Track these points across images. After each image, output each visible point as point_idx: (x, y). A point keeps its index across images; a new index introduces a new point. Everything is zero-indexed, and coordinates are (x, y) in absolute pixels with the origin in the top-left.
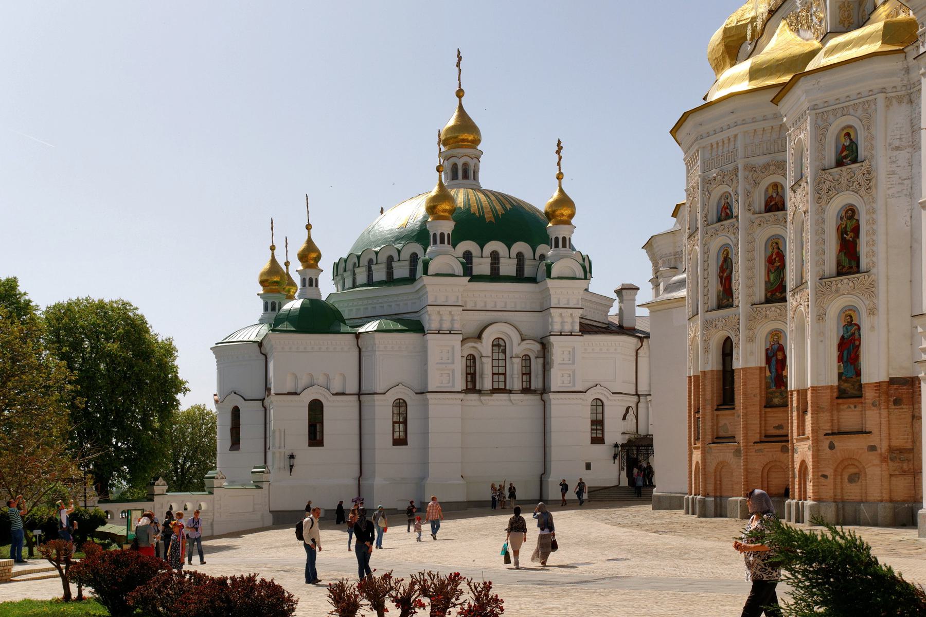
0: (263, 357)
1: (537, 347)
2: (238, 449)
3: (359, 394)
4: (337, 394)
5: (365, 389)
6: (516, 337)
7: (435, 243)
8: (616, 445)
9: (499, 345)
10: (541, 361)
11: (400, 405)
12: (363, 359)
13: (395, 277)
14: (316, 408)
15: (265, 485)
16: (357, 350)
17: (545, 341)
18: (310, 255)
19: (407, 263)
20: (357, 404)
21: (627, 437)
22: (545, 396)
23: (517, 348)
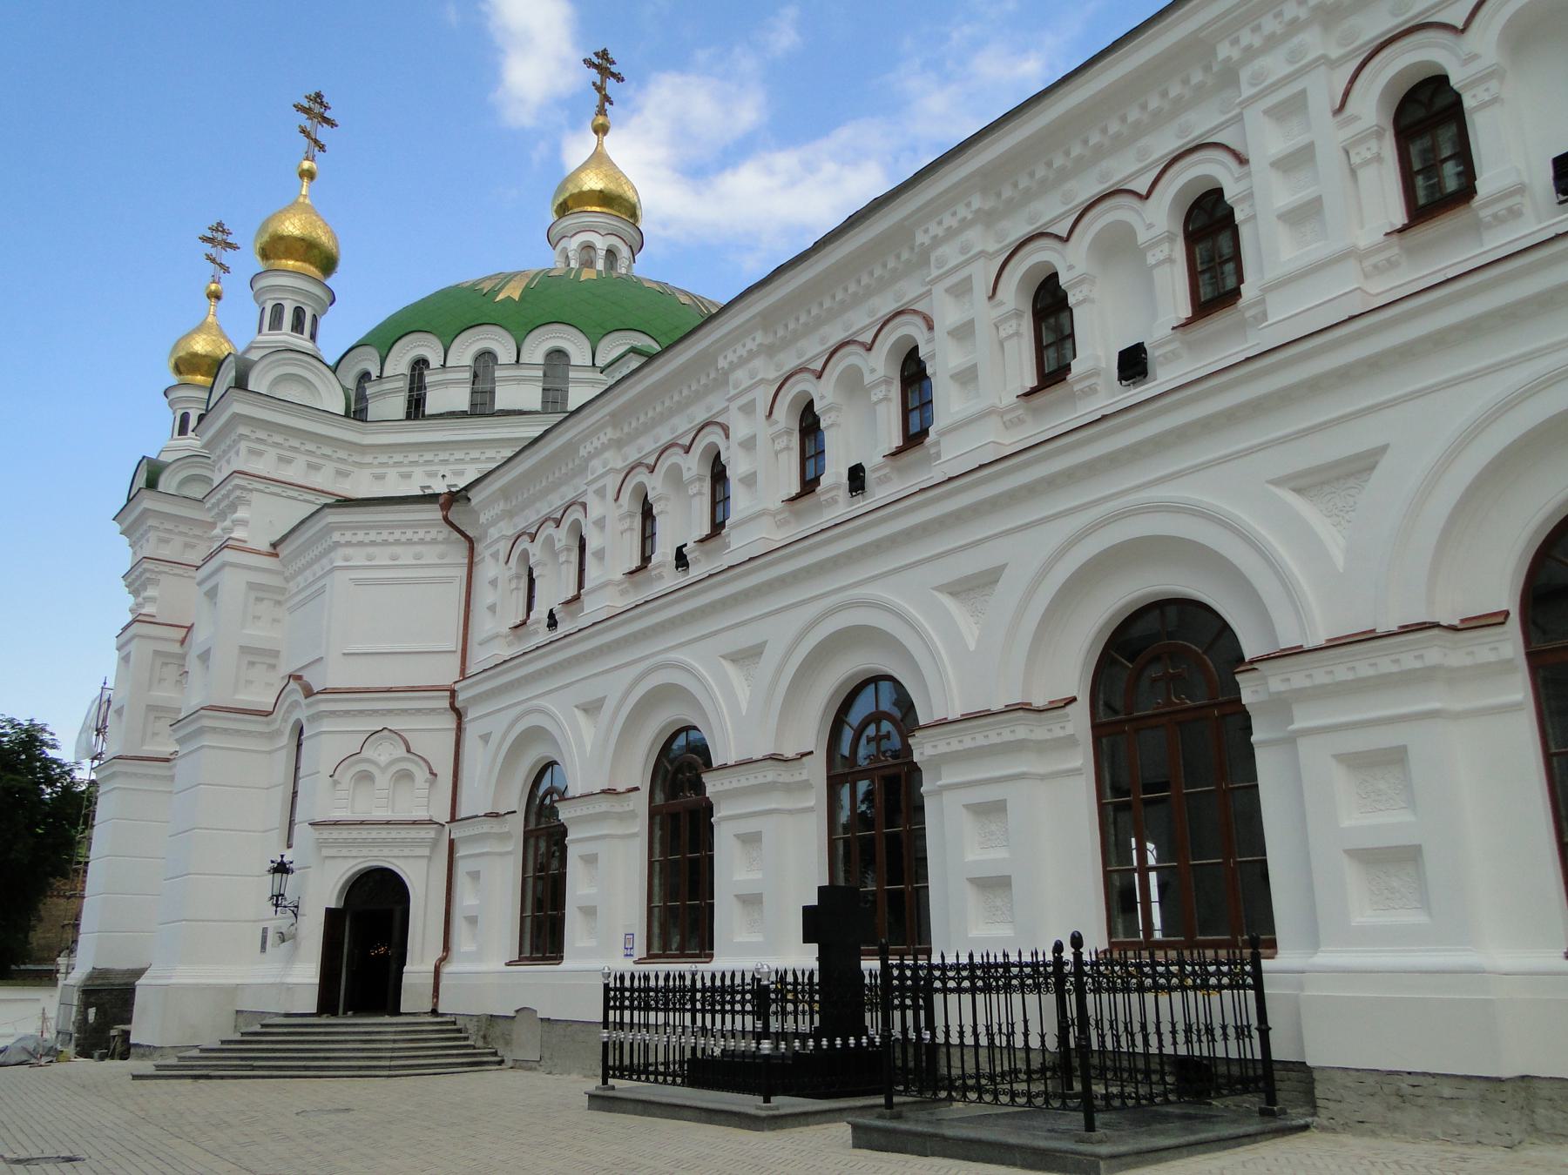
19: (541, 373)
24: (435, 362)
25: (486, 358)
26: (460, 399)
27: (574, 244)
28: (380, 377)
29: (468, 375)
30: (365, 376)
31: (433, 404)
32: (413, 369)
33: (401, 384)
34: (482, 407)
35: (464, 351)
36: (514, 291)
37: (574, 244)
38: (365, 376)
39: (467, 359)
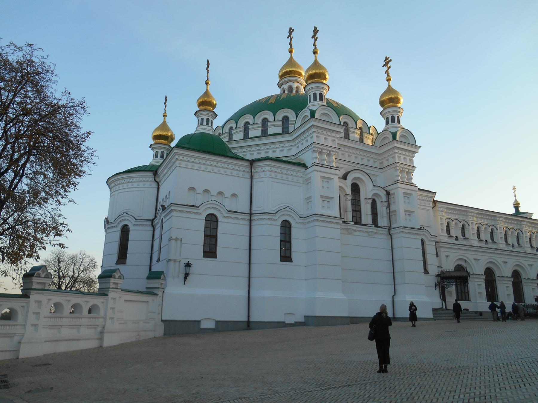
0: (155, 185)
1: (383, 194)
2: (124, 263)
3: (251, 214)
4: (230, 211)
5: (255, 209)
6: (370, 186)
7: (315, 99)
8: (438, 276)
9: (355, 188)
10: (386, 204)
11: (286, 227)
12: (254, 184)
13: (270, 132)
14: (212, 221)
15: (160, 294)
16: (248, 175)
17: (388, 189)
18: (206, 104)
19: (281, 123)
20: (248, 223)
21: (440, 269)
22: (392, 232)
23: (367, 191)
24: (251, 123)
25: (265, 120)
26: (258, 132)
27: (286, 87)
28: (236, 128)
29: (260, 125)
30: (231, 128)
31: (252, 134)
32: (245, 125)
33: (241, 129)
34: (265, 133)
35: (259, 118)
36: (272, 101)
37: (286, 87)
38: (231, 128)
39: (260, 121)
